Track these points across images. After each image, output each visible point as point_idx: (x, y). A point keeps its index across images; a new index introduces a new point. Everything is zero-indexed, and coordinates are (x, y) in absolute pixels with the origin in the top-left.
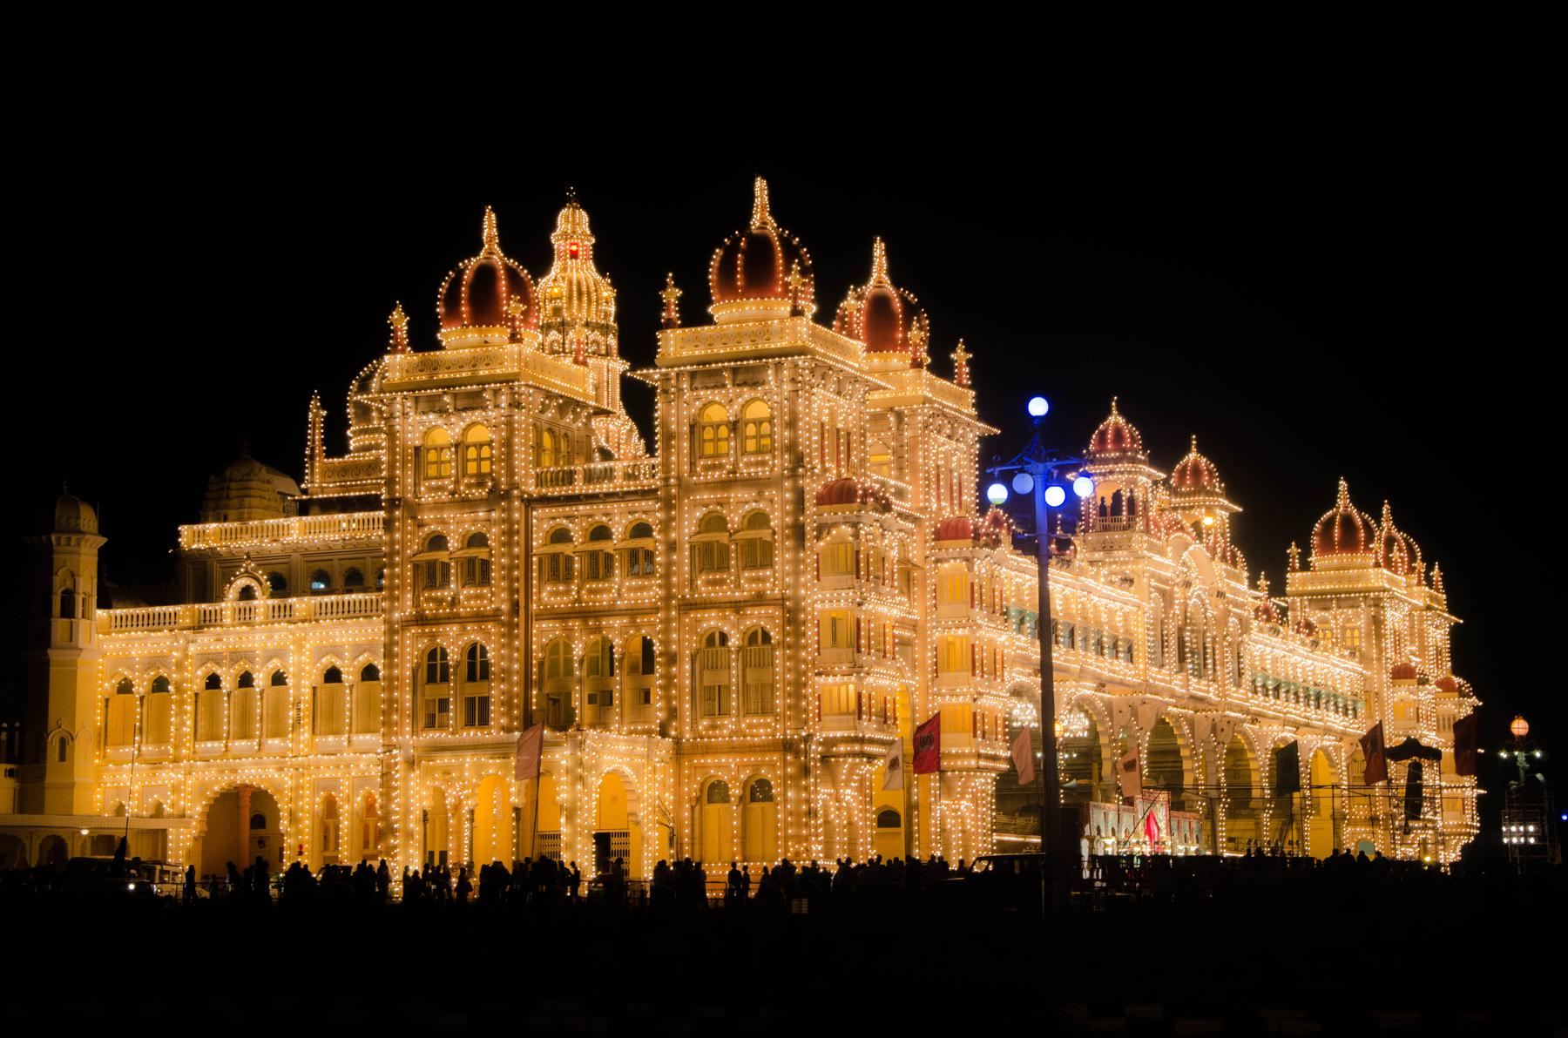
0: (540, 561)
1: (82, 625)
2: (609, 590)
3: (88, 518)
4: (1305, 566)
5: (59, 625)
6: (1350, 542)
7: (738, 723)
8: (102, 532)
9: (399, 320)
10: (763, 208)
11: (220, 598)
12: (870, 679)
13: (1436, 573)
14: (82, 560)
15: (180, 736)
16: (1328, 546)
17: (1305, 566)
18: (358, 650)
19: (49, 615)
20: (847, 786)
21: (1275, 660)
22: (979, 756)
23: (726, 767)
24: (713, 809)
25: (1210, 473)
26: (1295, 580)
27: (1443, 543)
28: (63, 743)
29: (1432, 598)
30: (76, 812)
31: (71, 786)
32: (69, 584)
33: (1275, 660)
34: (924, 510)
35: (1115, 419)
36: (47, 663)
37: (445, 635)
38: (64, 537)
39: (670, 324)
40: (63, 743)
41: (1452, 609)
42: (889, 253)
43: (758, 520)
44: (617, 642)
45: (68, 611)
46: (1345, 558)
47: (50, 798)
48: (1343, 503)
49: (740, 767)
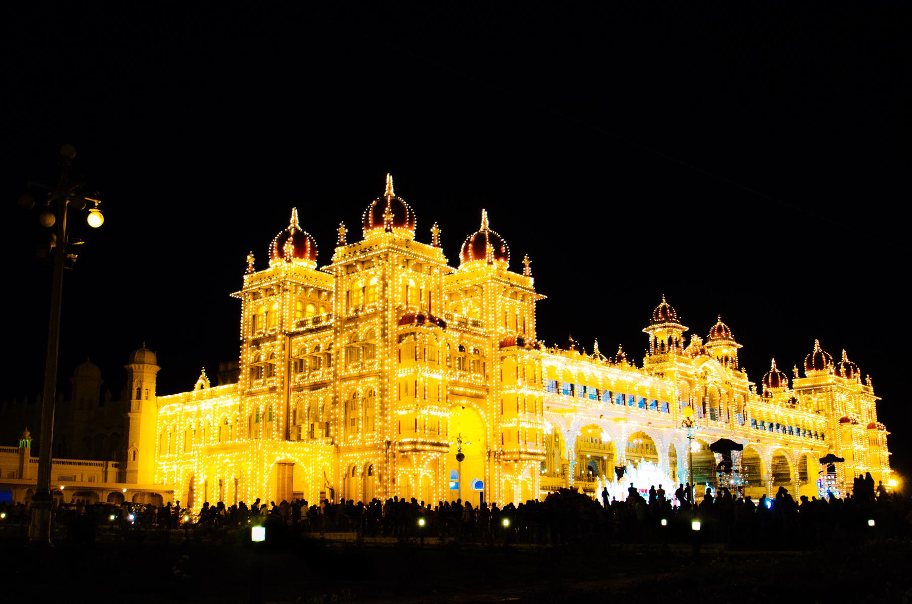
0: (296, 363)
1: (143, 401)
2: (318, 375)
3: (150, 357)
4: (802, 375)
5: (134, 402)
6: (819, 366)
7: (362, 436)
8: (158, 364)
9: (250, 259)
10: (390, 188)
11: (191, 388)
12: (424, 412)
13: (868, 380)
14: (147, 375)
15: (179, 449)
16: (810, 367)
17: (802, 375)
18: (234, 408)
19: (131, 398)
20: (417, 467)
21: (768, 414)
22: (520, 453)
23: (355, 458)
24: (353, 479)
25: (726, 331)
26: (797, 382)
27: (868, 364)
28: (135, 453)
29: (864, 389)
30: (139, 481)
31: (136, 471)
32: (139, 386)
33: (768, 414)
34: (491, 332)
35: (664, 303)
36: (129, 419)
37: (258, 400)
38: (137, 366)
39: (342, 244)
40: (135, 453)
41: (876, 393)
42: (490, 217)
43: (371, 334)
44: (321, 399)
45: (139, 397)
46: (819, 372)
47: (129, 476)
48: (817, 348)
49: (362, 458)
